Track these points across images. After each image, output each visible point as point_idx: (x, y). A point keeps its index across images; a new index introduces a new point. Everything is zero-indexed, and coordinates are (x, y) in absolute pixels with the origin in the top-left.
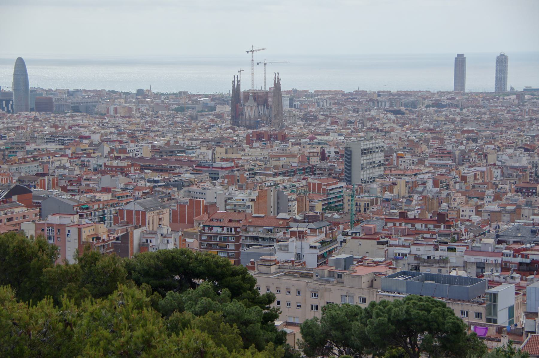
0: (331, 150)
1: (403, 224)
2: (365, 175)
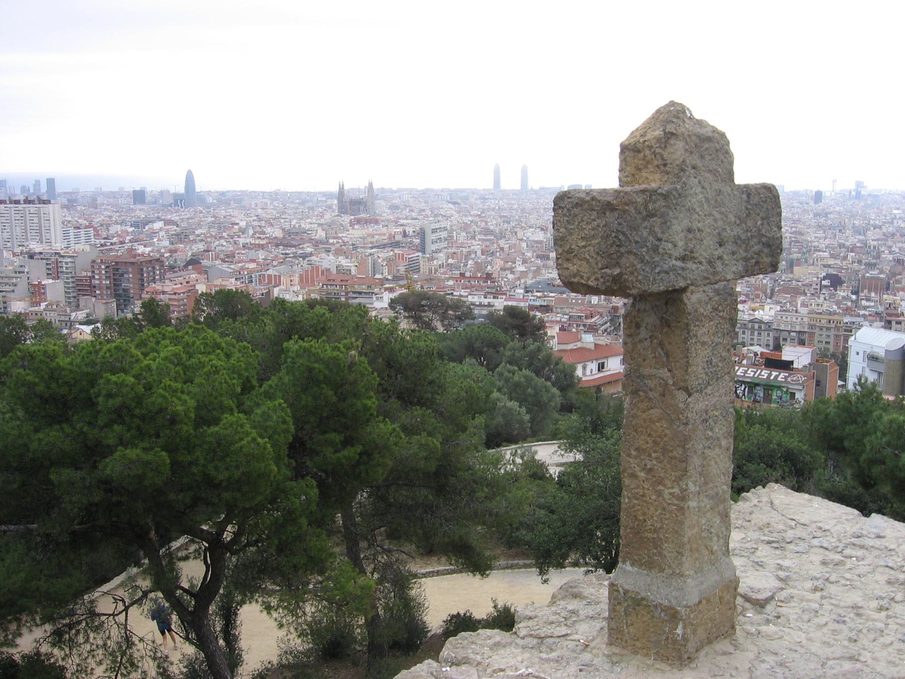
0: (410, 230)
2: (434, 247)
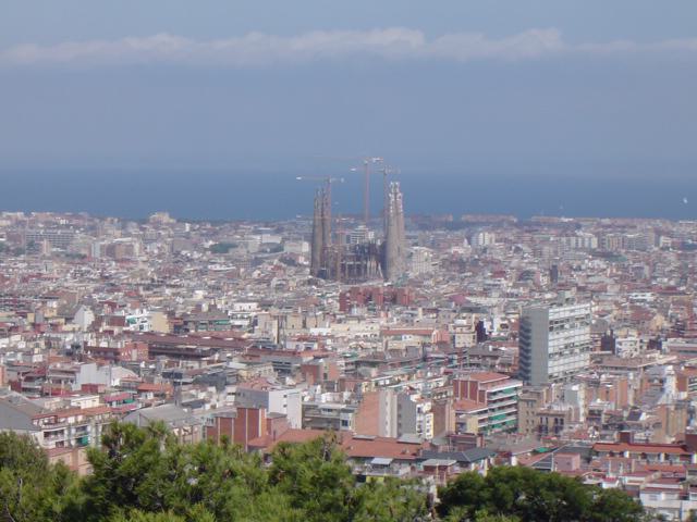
0: (494, 326)
1: (627, 455)
2: (556, 367)
